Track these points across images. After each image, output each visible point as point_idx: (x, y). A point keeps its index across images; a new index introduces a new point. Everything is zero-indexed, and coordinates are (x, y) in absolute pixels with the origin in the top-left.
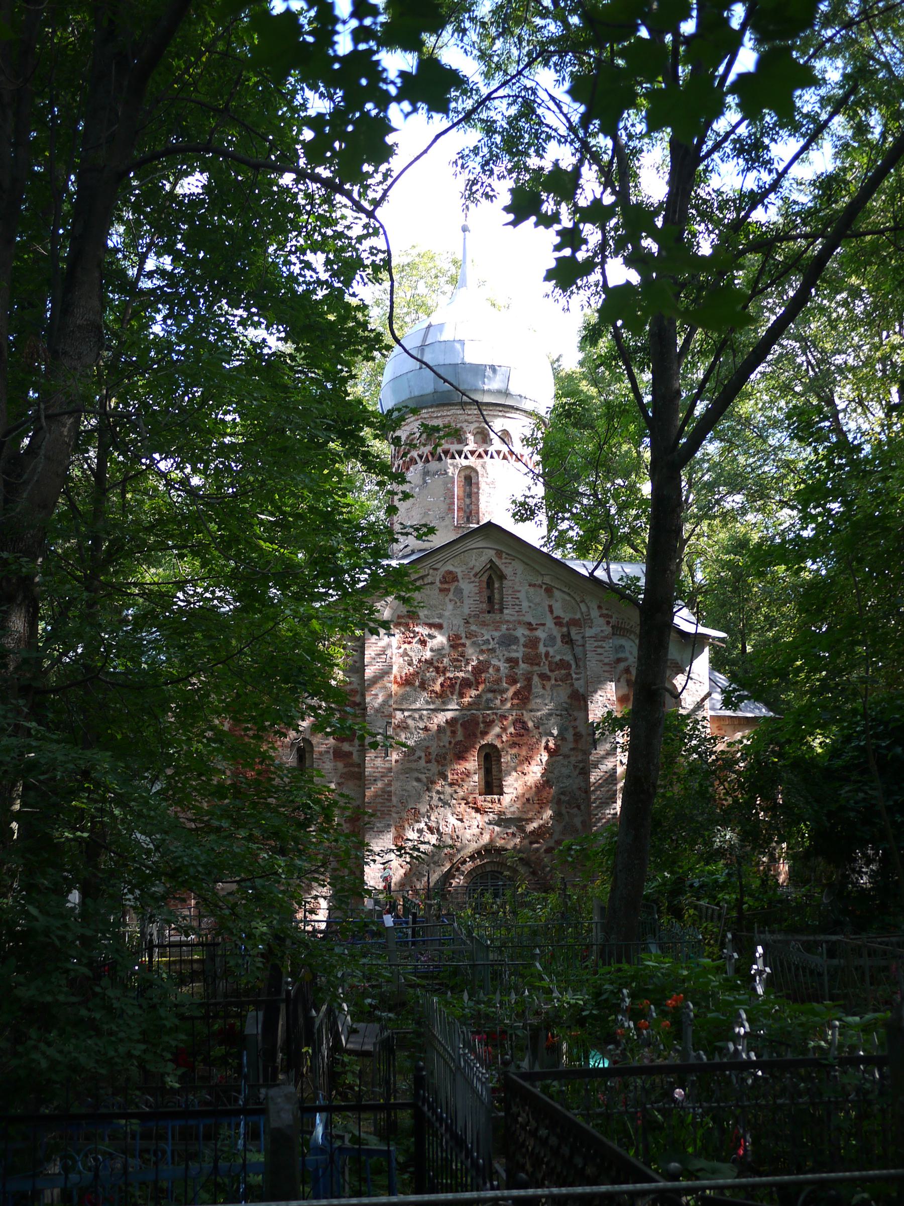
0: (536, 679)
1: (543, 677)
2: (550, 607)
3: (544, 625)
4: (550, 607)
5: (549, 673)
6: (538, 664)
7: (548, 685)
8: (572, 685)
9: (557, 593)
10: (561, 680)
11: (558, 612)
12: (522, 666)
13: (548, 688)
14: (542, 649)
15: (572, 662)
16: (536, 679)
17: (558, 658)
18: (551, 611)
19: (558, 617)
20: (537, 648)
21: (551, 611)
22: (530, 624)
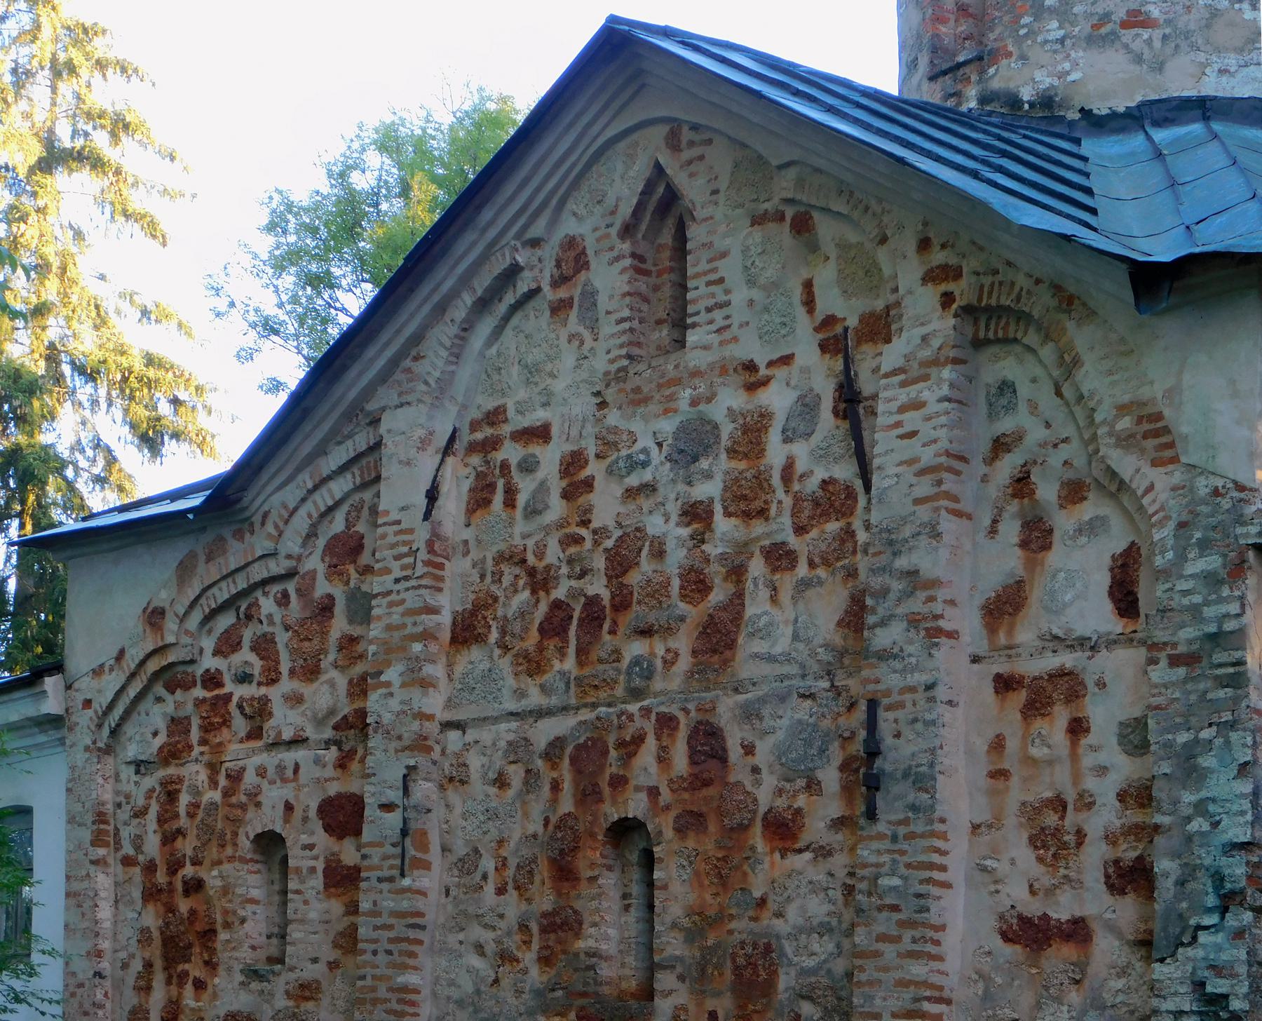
0: (757, 567)
1: (779, 557)
2: (808, 285)
3: (786, 360)
4: (808, 285)
5: (793, 541)
6: (762, 513)
7: (787, 582)
8: (852, 573)
9: (826, 230)
10: (826, 563)
11: (831, 301)
12: (723, 525)
13: (785, 596)
14: (776, 452)
15: (858, 484)
16: (757, 567)
17: (820, 474)
18: (809, 303)
19: (830, 321)
20: (761, 453)
21: (809, 303)
22: (750, 367)
